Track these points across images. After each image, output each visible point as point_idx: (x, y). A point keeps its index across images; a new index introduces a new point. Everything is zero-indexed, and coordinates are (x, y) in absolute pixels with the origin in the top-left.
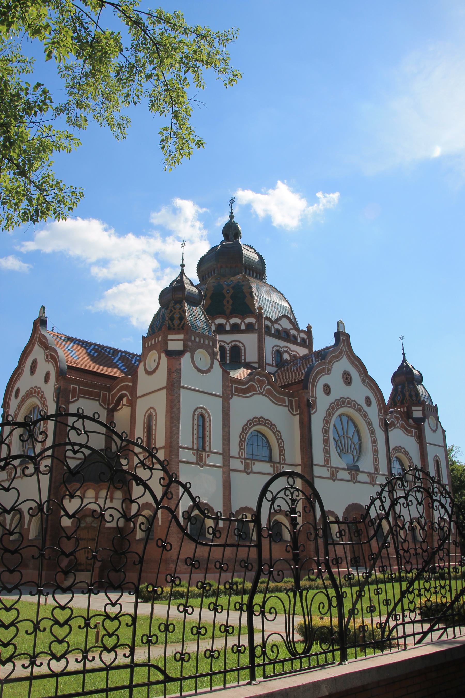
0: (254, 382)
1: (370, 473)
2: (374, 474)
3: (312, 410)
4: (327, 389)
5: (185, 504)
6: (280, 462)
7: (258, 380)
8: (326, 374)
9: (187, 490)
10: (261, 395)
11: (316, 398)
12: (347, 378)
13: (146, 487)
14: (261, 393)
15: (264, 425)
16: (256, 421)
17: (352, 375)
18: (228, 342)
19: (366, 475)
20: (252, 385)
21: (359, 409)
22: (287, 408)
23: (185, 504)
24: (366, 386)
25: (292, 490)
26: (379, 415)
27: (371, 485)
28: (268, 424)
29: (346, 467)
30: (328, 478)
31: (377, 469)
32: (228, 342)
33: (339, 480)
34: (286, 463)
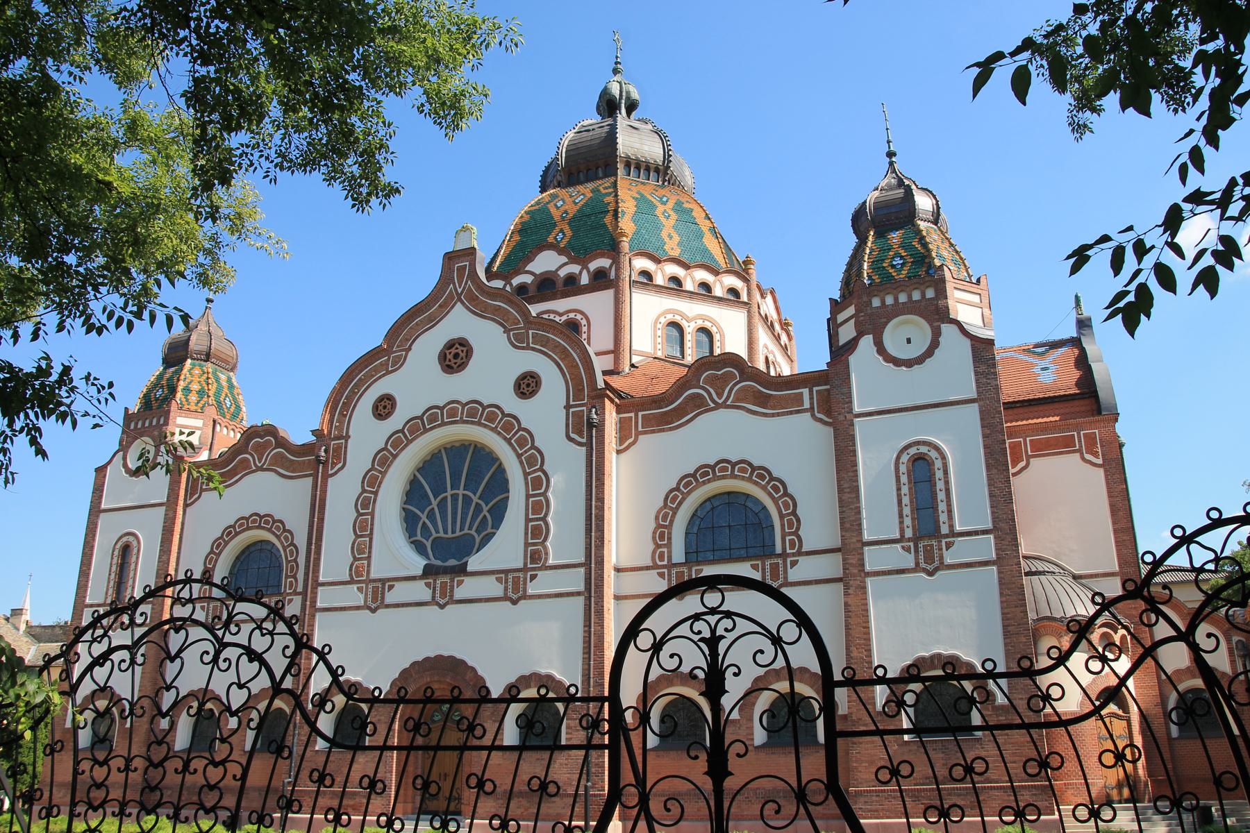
1: (506, 572)
2: (524, 569)
5: (320, 681)
8: (389, 373)
9: (322, 656)
12: (456, 356)
13: (264, 664)
16: (254, 521)
19: (493, 578)
20: (247, 460)
23: (320, 681)
24: (528, 348)
25: (713, 619)
28: (267, 522)
30: (358, 608)
33: (388, 606)
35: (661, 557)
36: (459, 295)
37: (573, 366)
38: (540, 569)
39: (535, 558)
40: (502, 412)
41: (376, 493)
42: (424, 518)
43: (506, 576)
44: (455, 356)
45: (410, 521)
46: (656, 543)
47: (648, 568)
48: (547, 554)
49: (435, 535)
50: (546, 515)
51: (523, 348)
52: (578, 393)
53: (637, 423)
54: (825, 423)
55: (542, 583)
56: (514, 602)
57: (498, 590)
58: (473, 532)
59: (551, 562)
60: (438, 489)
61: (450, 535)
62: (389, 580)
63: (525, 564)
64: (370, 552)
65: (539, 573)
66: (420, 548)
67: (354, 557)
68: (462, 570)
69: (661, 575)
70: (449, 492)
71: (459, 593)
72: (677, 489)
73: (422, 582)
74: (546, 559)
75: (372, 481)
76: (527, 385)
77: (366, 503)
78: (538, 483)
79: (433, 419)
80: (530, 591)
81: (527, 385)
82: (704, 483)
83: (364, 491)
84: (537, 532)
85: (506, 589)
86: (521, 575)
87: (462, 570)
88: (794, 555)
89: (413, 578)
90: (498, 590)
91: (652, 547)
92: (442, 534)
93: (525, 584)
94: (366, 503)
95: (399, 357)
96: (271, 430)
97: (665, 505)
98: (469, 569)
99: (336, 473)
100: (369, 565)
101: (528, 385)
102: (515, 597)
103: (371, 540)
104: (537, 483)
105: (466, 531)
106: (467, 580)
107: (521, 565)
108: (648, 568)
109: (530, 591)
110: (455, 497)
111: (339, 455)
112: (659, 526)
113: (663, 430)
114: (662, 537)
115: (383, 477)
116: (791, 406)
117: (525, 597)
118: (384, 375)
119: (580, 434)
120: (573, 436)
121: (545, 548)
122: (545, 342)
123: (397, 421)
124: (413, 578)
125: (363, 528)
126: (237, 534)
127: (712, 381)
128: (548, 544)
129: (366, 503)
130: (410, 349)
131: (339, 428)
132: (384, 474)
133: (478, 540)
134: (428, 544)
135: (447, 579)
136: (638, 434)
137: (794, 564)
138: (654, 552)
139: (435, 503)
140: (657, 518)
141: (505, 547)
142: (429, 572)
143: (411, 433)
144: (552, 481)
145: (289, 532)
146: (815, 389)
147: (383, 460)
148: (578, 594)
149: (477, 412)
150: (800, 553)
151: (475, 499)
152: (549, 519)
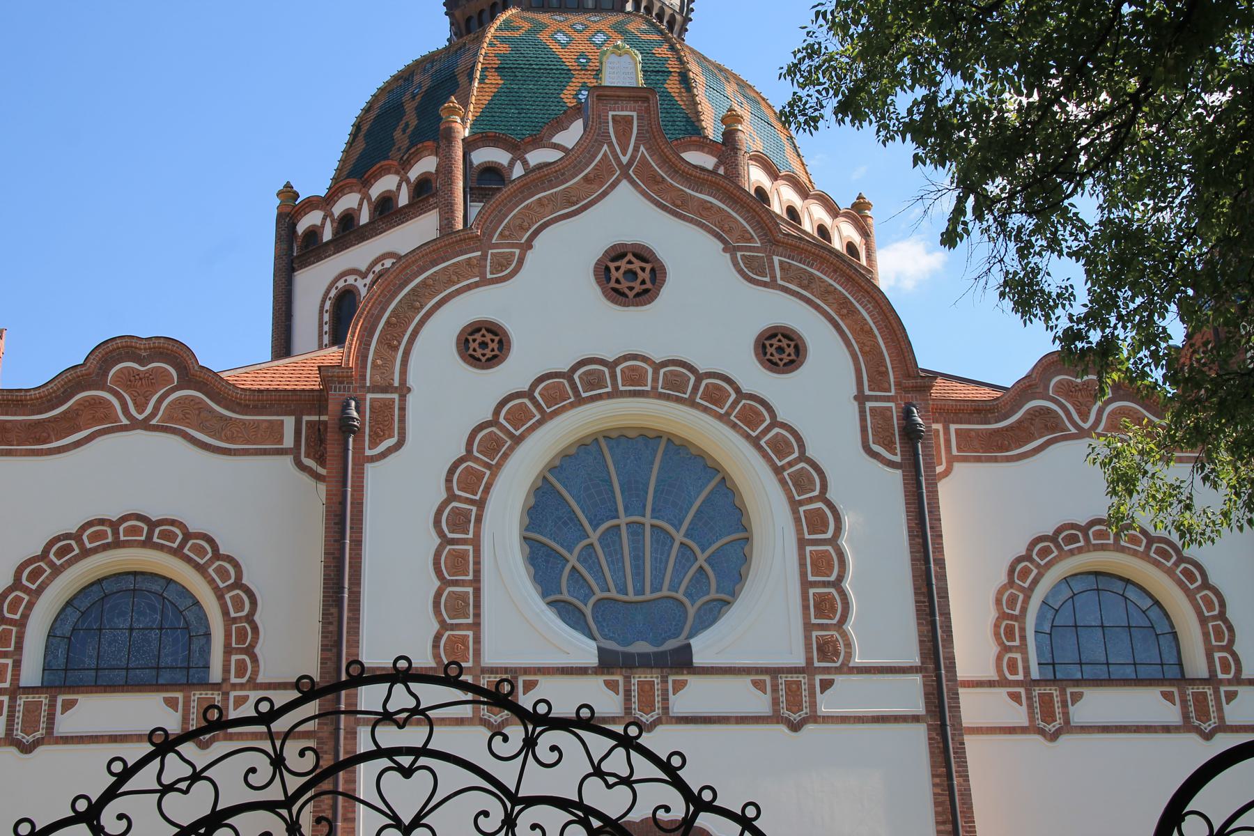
0: (103, 387)
1: (774, 672)
2: (808, 669)
3: (373, 444)
4: (484, 345)
6: (226, 679)
7: (129, 380)
8: (484, 282)
10: (139, 435)
11: (404, 390)
14: (145, 425)
15: (148, 543)
17: (663, 253)
18: (363, 268)
19: (746, 681)
21: (713, 392)
22: (288, 460)
24: (772, 285)
26: (861, 398)
27: (783, 729)
29: (593, 661)
31: (826, 650)
32: (363, 268)
34: (261, 679)
35: (1012, 667)
36: (625, 169)
37: (863, 331)
38: (839, 670)
39: (828, 652)
40: (738, 390)
41: (481, 504)
42: (573, 560)
43: (774, 679)
44: (630, 276)
45: (543, 563)
46: (1001, 644)
47: (991, 684)
48: (848, 645)
49: (599, 594)
50: (841, 578)
51: (765, 285)
52: (878, 378)
53: (948, 441)
54: (318, 477)
55: (843, 696)
56: (795, 727)
57: (760, 703)
58: (680, 595)
59: (857, 660)
60: (602, 510)
61: (631, 597)
62: (526, 671)
63: (809, 660)
64: (477, 615)
65: (839, 679)
66: (570, 614)
67: (442, 623)
68: (682, 661)
69: (1015, 697)
70: (623, 520)
71: (681, 704)
72: (1028, 557)
73: (599, 681)
74: (849, 655)
75: (469, 481)
76: (780, 349)
77: (459, 521)
78: (817, 520)
79: (593, 381)
80: (823, 709)
81: (780, 349)
82: (1072, 553)
83: (452, 497)
84: (824, 603)
85: (776, 702)
86: (802, 678)
87: (682, 661)
88: (1229, 682)
89: (582, 671)
90: (760, 703)
91: (994, 649)
92: (614, 594)
93: (812, 694)
94: (458, 520)
95: (508, 259)
96: (172, 352)
97: (1011, 583)
98: (698, 660)
99: (383, 455)
100: (477, 641)
101: (780, 350)
102: (796, 717)
103: (477, 592)
104: (816, 522)
105: (665, 592)
106: (693, 681)
107: (800, 661)
108: (991, 684)
109: (823, 709)
110: (636, 529)
111: (389, 424)
112: (1003, 616)
113: (995, 460)
114: (1010, 633)
115: (494, 476)
116: (261, 443)
117: (814, 718)
118: (477, 285)
119: (890, 447)
120: (876, 448)
121: (845, 635)
122: (808, 282)
123: (515, 373)
124: (582, 671)
125: (457, 568)
126: (86, 553)
127: (1068, 390)
128: (849, 627)
129: (459, 521)
130: (529, 245)
131: (384, 368)
132: (495, 470)
133: (692, 611)
134: (588, 611)
135: (654, 677)
136: (951, 460)
137: (1231, 696)
138: (999, 659)
139: (594, 537)
140: (998, 602)
141: (761, 624)
142: (608, 663)
143: (550, 401)
144: (847, 521)
145: (230, 559)
146: (306, 418)
147: (491, 443)
148: (916, 719)
149: (680, 381)
150: (1238, 680)
151: (679, 537)
152: (847, 585)
